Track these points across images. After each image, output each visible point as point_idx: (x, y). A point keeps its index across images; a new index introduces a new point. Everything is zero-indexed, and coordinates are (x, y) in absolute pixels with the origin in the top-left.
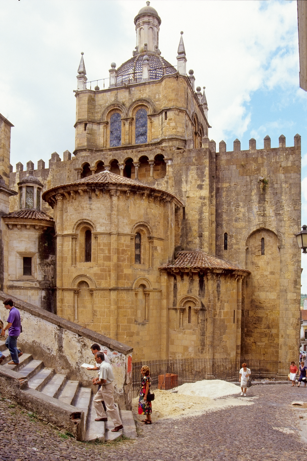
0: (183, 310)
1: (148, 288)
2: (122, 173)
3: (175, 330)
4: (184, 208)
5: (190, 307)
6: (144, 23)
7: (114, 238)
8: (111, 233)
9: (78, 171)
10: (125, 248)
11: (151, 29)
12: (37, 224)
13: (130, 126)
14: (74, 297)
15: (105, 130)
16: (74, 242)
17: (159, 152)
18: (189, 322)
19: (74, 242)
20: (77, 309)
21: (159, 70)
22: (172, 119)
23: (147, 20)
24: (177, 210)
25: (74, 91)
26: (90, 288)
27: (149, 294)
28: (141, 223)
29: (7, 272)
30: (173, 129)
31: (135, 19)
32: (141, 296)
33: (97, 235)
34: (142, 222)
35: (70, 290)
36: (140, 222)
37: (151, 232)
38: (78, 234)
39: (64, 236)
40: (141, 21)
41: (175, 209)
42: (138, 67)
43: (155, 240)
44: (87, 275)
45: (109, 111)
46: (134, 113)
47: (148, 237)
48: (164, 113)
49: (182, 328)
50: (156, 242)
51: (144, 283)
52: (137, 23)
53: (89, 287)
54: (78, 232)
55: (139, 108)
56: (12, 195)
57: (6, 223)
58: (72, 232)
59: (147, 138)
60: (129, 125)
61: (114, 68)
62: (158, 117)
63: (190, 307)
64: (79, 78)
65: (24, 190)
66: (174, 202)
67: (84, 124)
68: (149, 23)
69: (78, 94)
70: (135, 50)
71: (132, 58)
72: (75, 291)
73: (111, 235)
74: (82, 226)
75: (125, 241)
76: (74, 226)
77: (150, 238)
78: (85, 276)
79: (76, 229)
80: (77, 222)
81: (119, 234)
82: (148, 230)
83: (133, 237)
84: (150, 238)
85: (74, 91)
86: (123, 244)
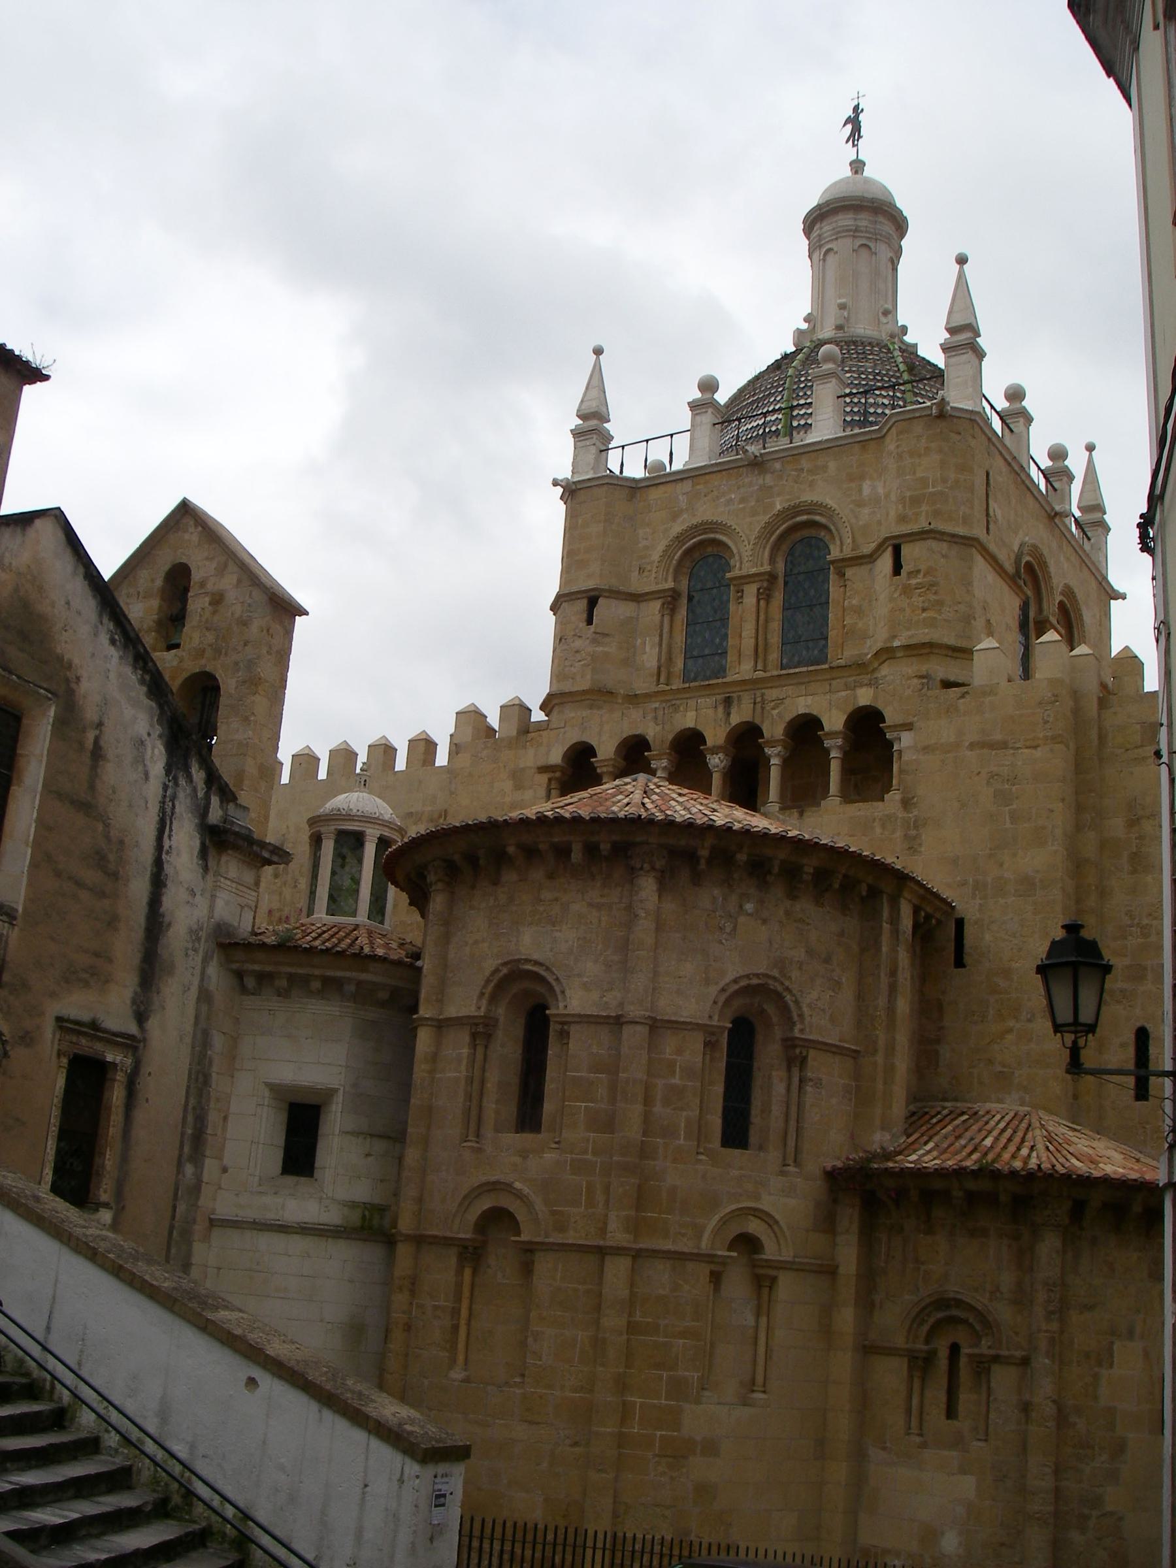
0: (921, 1364)
1: (771, 1251)
2: (717, 780)
3: (884, 1449)
4: (960, 923)
5: (955, 1349)
6: (838, 235)
7: (634, 1036)
8: (621, 1016)
10: (676, 1081)
11: (864, 252)
12: (348, 974)
13: (762, 603)
14: (459, 1272)
15: (667, 619)
16: (480, 1051)
17: (864, 697)
18: (951, 1413)
19: (480, 1051)
20: (469, 1324)
21: (884, 393)
22: (918, 571)
23: (851, 222)
24: (924, 933)
25: (556, 483)
26: (524, 1237)
27: (774, 1280)
28: (755, 981)
29: (220, 1158)
30: (924, 610)
32: (737, 1285)
34: (757, 975)
35: (447, 1242)
36: (748, 976)
37: (796, 1018)
38: (497, 1020)
39: (441, 1025)
40: (826, 228)
41: (916, 926)
42: (802, 385)
43: (812, 1053)
44: (518, 1185)
45: (684, 548)
47: (785, 1040)
48: (889, 551)
49: (918, 1439)
50: (821, 1067)
51: (754, 1227)
52: (814, 234)
53: (518, 1233)
54: (501, 1011)
55: (798, 536)
56: (269, 862)
57: (235, 966)
58: (473, 1008)
59: (826, 646)
60: (758, 601)
61: (708, 396)
62: (870, 566)
63: (955, 1349)
64: (577, 434)
65: (328, 847)
66: (906, 894)
67: (585, 602)
68: (856, 231)
69: (571, 492)
70: (805, 326)
71: (786, 356)
72: (466, 1248)
73: (622, 1024)
75: (679, 1051)
76: (485, 987)
77: (790, 1043)
79: (493, 999)
80: (497, 971)
81: (656, 1026)
82: (784, 1009)
83: (714, 1039)
84: (790, 1043)
85: (556, 483)
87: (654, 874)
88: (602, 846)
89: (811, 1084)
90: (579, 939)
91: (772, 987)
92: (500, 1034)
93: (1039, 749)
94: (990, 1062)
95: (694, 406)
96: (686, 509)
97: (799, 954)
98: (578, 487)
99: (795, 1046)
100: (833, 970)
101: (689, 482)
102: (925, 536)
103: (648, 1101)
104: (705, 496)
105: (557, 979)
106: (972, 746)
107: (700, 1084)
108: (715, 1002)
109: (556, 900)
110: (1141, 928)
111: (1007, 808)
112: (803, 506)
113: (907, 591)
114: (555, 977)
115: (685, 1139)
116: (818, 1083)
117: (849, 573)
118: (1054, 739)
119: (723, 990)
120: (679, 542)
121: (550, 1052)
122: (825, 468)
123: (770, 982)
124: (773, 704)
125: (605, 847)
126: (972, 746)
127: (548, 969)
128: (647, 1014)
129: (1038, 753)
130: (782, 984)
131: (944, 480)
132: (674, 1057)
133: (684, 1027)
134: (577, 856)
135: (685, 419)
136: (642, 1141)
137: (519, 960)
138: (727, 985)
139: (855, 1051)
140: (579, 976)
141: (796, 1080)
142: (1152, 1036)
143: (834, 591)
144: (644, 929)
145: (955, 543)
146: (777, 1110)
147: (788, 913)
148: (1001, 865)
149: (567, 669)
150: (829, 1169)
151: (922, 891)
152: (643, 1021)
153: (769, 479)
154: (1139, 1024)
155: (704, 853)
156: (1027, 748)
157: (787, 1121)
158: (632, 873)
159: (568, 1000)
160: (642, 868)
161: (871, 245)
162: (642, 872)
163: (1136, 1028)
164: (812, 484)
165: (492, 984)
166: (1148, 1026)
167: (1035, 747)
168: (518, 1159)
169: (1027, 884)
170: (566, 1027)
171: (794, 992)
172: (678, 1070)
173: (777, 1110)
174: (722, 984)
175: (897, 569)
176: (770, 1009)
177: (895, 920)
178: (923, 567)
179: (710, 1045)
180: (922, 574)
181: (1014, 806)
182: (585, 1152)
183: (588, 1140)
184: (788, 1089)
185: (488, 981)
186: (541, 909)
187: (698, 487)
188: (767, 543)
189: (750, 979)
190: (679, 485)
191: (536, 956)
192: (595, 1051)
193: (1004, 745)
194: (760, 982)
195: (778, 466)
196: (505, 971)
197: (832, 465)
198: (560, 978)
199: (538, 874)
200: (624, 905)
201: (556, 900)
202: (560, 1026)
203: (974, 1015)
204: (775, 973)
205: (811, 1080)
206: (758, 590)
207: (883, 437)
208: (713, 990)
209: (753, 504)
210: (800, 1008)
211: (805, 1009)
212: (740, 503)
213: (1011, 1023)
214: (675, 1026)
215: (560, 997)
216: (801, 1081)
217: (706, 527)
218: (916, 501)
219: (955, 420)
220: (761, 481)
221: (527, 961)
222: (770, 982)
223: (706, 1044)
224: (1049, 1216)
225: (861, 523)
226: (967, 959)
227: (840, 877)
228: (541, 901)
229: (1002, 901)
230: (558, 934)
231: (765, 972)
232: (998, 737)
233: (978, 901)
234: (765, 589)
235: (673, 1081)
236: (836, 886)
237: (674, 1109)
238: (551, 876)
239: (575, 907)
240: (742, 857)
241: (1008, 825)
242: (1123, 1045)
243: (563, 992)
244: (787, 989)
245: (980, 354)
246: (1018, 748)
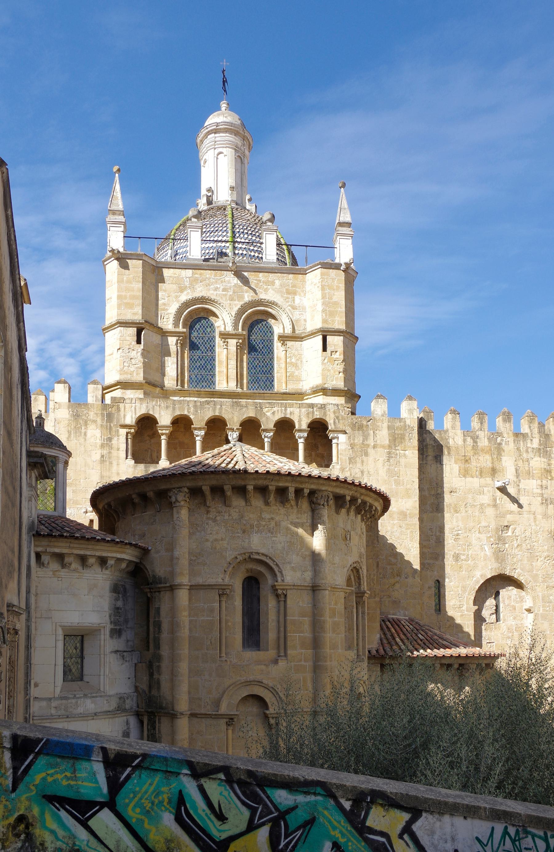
9: (128, 430)
10: (336, 619)
60: (237, 349)
62: (300, 343)
74: (243, 568)
75: (336, 604)
78: (259, 683)
80: (236, 558)
105: (277, 565)
109: (272, 519)
124: (267, 409)
125: (306, 491)
127: (270, 558)
137: (252, 553)
140: (289, 563)
149: (126, 368)
168: (263, 667)
175: (325, 349)
182: (301, 661)
183: (302, 654)
186: (264, 523)
191: (263, 551)
196: (240, 558)
201: (272, 519)
206: (237, 343)
215: (278, 574)
221: (258, 553)
228: (263, 519)
229: (392, 522)
230: (274, 539)
234: (241, 344)
241: (394, 486)
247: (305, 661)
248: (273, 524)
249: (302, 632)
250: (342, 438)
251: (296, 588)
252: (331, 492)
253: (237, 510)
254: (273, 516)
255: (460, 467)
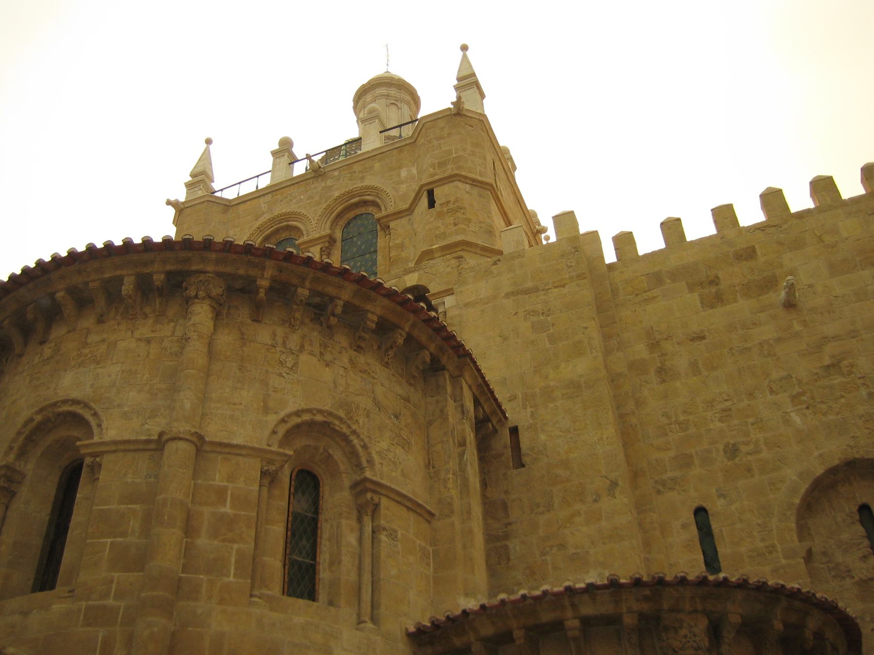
4: (514, 431)
10: (227, 509)
11: (393, 108)
25: (169, 203)
28: (319, 418)
30: (455, 225)
31: (354, 101)
33: (101, 454)
34: (320, 411)
36: (309, 411)
43: (384, 501)
45: (263, 235)
46: (338, 227)
48: (426, 193)
62: (408, 217)
66: (467, 375)
75: (231, 478)
77: (361, 487)
80: (31, 420)
82: (353, 455)
83: (273, 468)
84: (361, 487)
85: (169, 203)
86: (221, 494)
87: (209, 302)
88: (155, 277)
89: (385, 533)
90: (123, 372)
91: (338, 428)
92: (24, 492)
93: (567, 286)
94: (562, 546)
95: (274, 153)
96: (267, 212)
97: (365, 402)
98: (186, 206)
99: (366, 490)
100: (401, 429)
101: (270, 195)
102: (452, 179)
103: (189, 529)
104: (281, 201)
105: (95, 414)
106: (507, 296)
107: (255, 514)
108: (274, 432)
109: (103, 341)
110: (679, 424)
111: (545, 334)
112: (355, 191)
113: (440, 215)
114: (93, 412)
115: (235, 576)
116: (393, 535)
117: (392, 225)
118: (579, 277)
119: (283, 421)
120: (260, 231)
121: (78, 495)
122: (371, 168)
123: (337, 422)
125: (159, 279)
126: (507, 296)
127: (86, 406)
128: (193, 430)
129: (565, 290)
130: (349, 427)
131: (464, 150)
132: (226, 484)
133: (237, 451)
134: (128, 286)
135: (268, 163)
136: (180, 579)
137: (55, 405)
138: (289, 416)
139: (432, 515)
141: (368, 529)
142: (710, 512)
143: (381, 242)
144: (196, 350)
145: (475, 185)
146: (347, 561)
147: (351, 361)
148: (547, 377)
150: (412, 629)
151: (480, 380)
152: (188, 437)
153: (329, 183)
154: (696, 505)
155: (264, 283)
156: (556, 287)
157: (360, 575)
158: (187, 301)
159: (104, 431)
160: (196, 297)
161: (399, 105)
162: (197, 300)
163: (694, 508)
164: (363, 178)
165: (24, 436)
166: (704, 505)
167: (563, 286)
169: (574, 387)
170: (97, 459)
171: (362, 436)
172: (229, 498)
173: (347, 561)
174: (282, 414)
175: (432, 204)
176: (337, 454)
177: (458, 398)
178: (452, 199)
179: (269, 477)
180: (452, 203)
181: (552, 331)
183: (112, 582)
184: (360, 540)
185: (19, 433)
186: (86, 351)
187: (276, 197)
188: (328, 219)
189: (314, 415)
190: (262, 199)
191: (75, 395)
192: (130, 480)
193: (536, 290)
194: (325, 419)
195: (336, 173)
197: (377, 165)
198: (99, 412)
199: (88, 322)
200: (175, 339)
201: (103, 341)
202: (92, 459)
203: (539, 507)
204: (342, 414)
205: (384, 529)
206: (321, 249)
207: (415, 141)
208: (272, 419)
209: (316, 199)
210: (369, 454)
211: (376, 458)
212: (308, 199)
213: (577, 507)
214: (227, 450)
216: (373, 532)
217: (282, 218)
218: (442, 164)
219: (468, 118)
220: (323, 185)
221: (65, 402)
222: (337, 422)
223: (264, 474)
224: (685, 636)
225: (400, 193)
226: (526, 460)
227: (404, 334)
228: (87, 344)
229: (551, 405)
230: (100, 371)
231: (330, 410)
232: (530, 284)
233: (529, 410)
234: (327, 248)
235: (223, 510)
236: (401, 341)
237: (223, 541)
238: (100, 321)
239: (122, 345)
240: (303, 292)
242: (684, 526)
243: (99, 426)
244: (354, 432)
245: (483, 96)
246: (548, 289)
247: (116, 598)
248: (103, 348)
249: (123, 534)
250: (449, 301)
251: (122, 447)
252: (219, 275)
253: (53, 345)
254: (105, 336)
255: (701, 296)
